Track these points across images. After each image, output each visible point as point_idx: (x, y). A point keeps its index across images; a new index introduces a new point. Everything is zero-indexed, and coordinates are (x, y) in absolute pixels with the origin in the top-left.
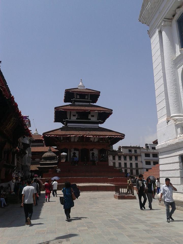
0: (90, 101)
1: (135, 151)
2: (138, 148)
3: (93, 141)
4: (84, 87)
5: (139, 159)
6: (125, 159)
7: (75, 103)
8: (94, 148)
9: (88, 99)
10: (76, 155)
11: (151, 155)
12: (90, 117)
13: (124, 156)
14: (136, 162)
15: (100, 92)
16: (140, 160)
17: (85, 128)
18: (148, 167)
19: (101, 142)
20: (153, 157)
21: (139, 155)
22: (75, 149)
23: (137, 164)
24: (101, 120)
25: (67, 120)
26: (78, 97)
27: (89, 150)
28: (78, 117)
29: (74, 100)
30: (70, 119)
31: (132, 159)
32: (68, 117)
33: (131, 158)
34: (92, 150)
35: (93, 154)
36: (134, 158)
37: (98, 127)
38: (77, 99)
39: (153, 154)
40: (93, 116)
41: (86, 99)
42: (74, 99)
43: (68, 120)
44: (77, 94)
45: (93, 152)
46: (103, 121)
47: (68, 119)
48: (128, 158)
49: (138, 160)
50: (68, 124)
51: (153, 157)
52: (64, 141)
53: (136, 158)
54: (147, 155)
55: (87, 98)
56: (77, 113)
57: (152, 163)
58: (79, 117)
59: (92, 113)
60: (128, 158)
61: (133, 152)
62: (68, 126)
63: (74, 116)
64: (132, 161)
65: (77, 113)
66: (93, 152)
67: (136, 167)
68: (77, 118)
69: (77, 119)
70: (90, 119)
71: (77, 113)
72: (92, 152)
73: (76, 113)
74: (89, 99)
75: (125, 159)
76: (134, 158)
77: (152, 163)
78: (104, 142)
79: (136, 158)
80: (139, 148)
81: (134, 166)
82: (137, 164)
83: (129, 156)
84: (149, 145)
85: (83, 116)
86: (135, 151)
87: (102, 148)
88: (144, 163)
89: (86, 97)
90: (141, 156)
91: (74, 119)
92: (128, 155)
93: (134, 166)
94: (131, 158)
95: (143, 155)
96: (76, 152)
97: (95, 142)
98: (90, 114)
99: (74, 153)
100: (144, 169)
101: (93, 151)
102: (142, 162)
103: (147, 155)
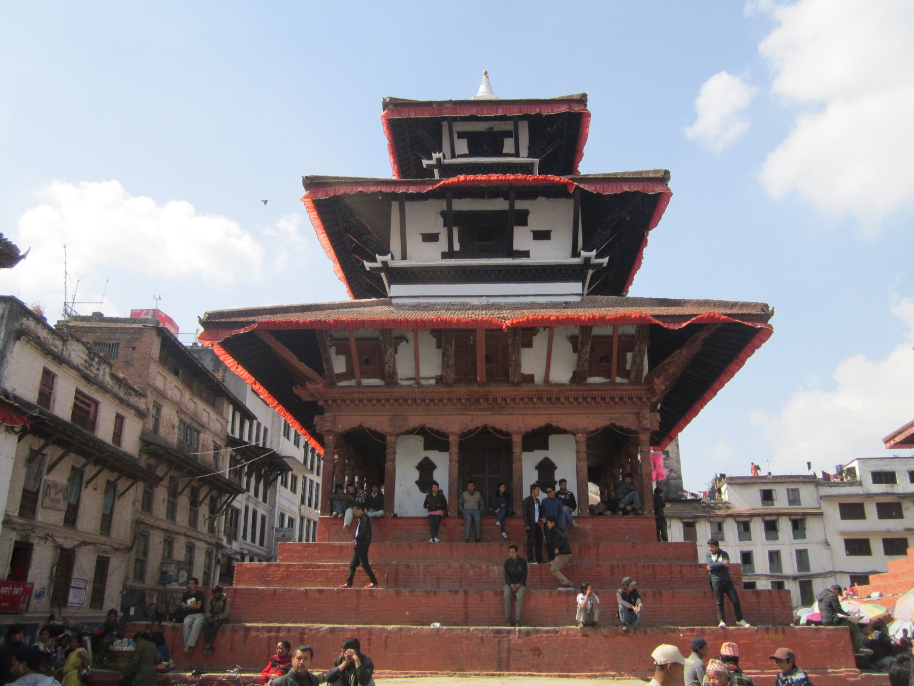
0: (532, 164)
1: (794, 498)
2: (803, 482)
3: (539, 378)
5: (812, 527)
6: (745, 528)
9: (517, 154)
11: (871, 510)
12: (522, 239)
13: (737, 522)
14: (800, 545)
15: (582, 100)
16: (822, 537)
18: (859, 564)
21: (809, 511)
23: (802, 557)
24: (594, 253)
26: (462, 146)
27: (517, 440)
29: (438, 160)
30: (404, 257)
31: (780, 534)
32: (395, 245)
33: (771, 528)
35: (546, 468)
36: (785, 526)
38: (453, 156)
40: (542, 235)
42: (435, 156)
43: (388, 258)
46: (606, 260)
48: (757, 528)
52: (353, 382)
53: (798, 525)
54: (852, 510)
55: (512, 151)
57: (877, 546)
58: (457, 247)
59: (536, 222)
60: (757, 528)
61: (781, 501)
63: (430, 238)
66: (546, 460)
67: (800, 569)
68: (446, 250)
69: (444, 256)
70: (526, 254)
72: (538, 456)
73: (441, 221)
74: (524, 151)
75: (745, 528)
76: (785, 526)
77: (877, 546)
78: (618, 380)
79: (798, 525)
80: (810, 480)
81: (789, 566)
82: (802, 557)
83: (763, 521)
84: (855, 464)
86: (794, 498)
87: (608, 423)
88: (839, 546)
89: (508, 145)
90: (821, 514)
91: (427, 255)
92: (758, 515)
93: (789, 566)
94: (771, 528)
95: (832, 512)
96: (436, 456)
98: (524, 223)
99: (426, 468)
100: (838, 576)
101: (545, 447)
102: (827, 543)
103: (852, 510)
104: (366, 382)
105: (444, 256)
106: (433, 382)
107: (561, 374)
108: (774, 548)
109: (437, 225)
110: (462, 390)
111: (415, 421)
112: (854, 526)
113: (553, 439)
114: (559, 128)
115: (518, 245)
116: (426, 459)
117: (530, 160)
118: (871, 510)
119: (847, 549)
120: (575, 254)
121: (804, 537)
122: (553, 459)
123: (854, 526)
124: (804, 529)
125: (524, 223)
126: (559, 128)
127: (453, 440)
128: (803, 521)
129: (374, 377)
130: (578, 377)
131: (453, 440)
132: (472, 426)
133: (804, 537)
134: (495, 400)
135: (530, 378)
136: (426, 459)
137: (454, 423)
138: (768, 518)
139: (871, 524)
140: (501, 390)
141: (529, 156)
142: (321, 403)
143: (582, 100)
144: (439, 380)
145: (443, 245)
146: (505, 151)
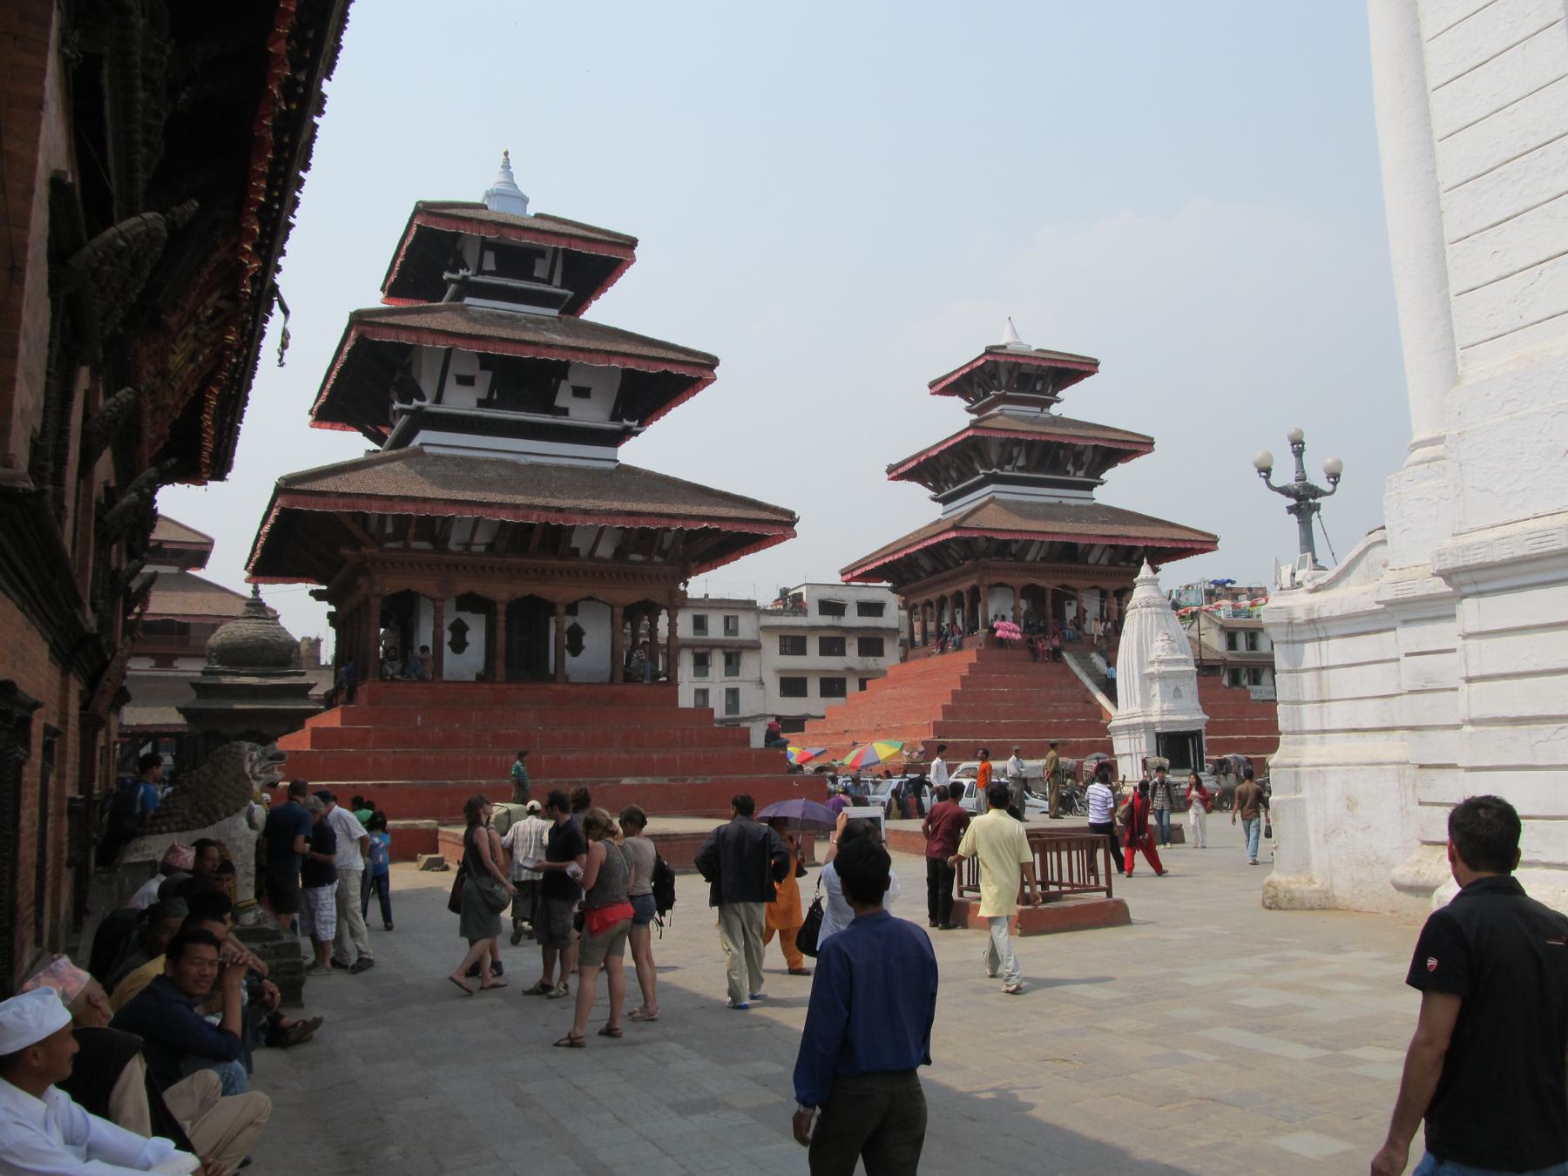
1: (730, 626)
2: (744, 609)
3: (583, 553)
4: (525, 200)
5: (749, 665)
7: (468, 301)
8: (589, 599)
9: (549, 282)
10: (469, 637)
11: (813, 645)
12: (563, 399)
15: (631, 243)
16: (755, 675)
17: (532, 466)
19: (635, 557)
20: (821, 654)
22: (469, 602)
23: (733, 694)
25: (420, 408)
26: (490, 263)
27: (561, 609)
28: (490, 393)
29: (465, 278)
30: (438, 400)
32: (428, 386)
33: (701, 663)
34: (572, 609)
36: (717, 661)
37: (611, 465)
38: (480, 272)
39: (822, 641)
40: (582, 393)
41: (538, 280)
42: (462, 272)
44: (486, 245)
45: (582, 620)
47: (422, 398)
49: (742, 670)
50: (423, 436)
51: (821, 654)
53: (732, 663)
54: (792, 644)
56: (483, 367)
59: (575, 379)
61: (716, 630)
62: (427, 449)
64: (708, 679)
65: (486, 362)
68: (484, 396)
69: (482, 403)
71: (486, 362)
72: (569, 621)
73: (477, 362)
74: (557, 280)
76: (717, 661)
77: (814, 687)
78: (657, 559)
80: (749, 606)
82: (733, 694)
84: (803, 590)
85: (524, 385)
86: (730, 626)
88: (773, 686)
89: (540, 269)
91: (461, 401)
94: (701, 663)
95: (771, 646)
96: (468, 617)
97: (601, 560)
98: (566, 378)
99: (459, 630)
102: (761, 683)
103: (792, 644)
104: (415, 545)
105: (482, 403)
106: (482, 549)
107: (605, 550)
108: (702, 686)
109: (472, 369)
110: (516, 561)
111: (463, 587)
112: (794, 662)
113: (581, 607)
114: (595, 260)
115: (560, 401)
116: (459, 621)
117: (565, 291)
118: (813, 645)
119: (782, 688)
120: (614, 417)
121: (737, 674)
122: (583, 625)
123: (794, 662)
124: (738, 664)
125: (566, 378)
126: (595, 260)
127: (501, 608)
128: (738, 655)
129: (422, 539)
130: (620, 553)
131: (501, 608)
132: (519, 595)
133: (737, 674)
134: (543, 571)
135: (576, 552)
136: (459, 621)
137: (502, 592)
138: (699, 650)
139: (813, 660)
140: (556, 563)
141: (562, 287)
142: (368, 564)
143: (631, 243)
144: (490, 547)
145: (481, 389)
146: (536, 274)
